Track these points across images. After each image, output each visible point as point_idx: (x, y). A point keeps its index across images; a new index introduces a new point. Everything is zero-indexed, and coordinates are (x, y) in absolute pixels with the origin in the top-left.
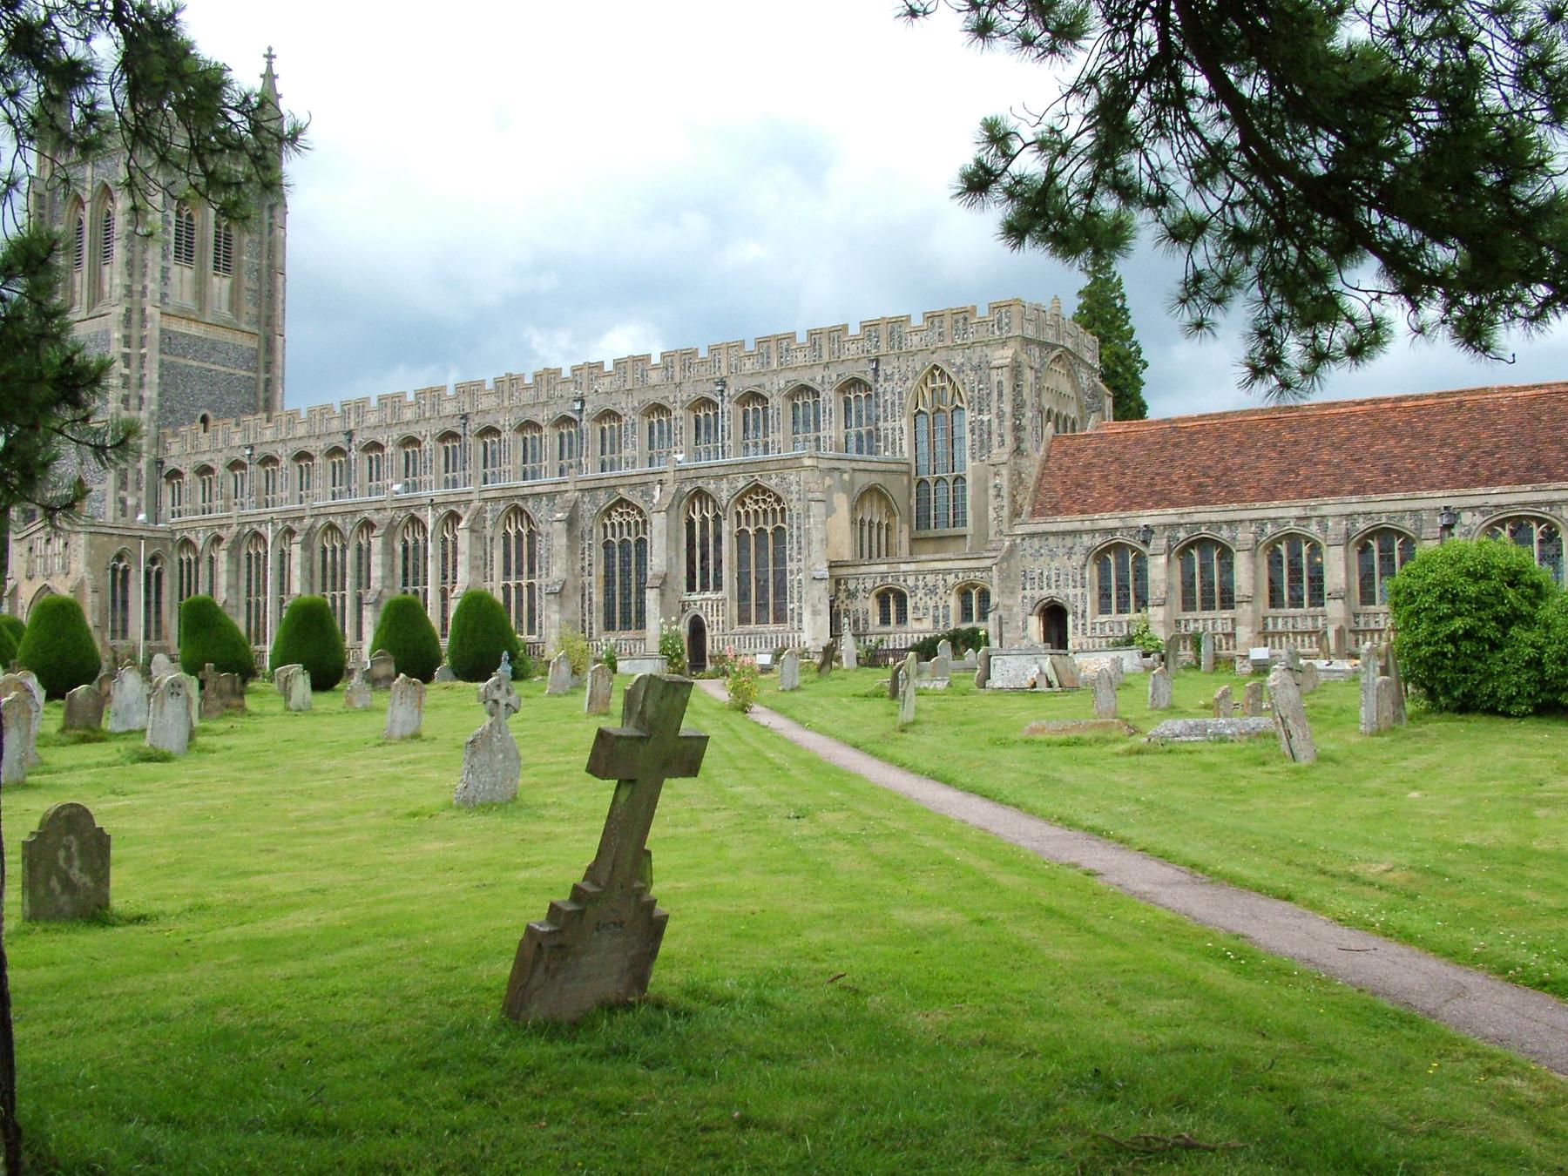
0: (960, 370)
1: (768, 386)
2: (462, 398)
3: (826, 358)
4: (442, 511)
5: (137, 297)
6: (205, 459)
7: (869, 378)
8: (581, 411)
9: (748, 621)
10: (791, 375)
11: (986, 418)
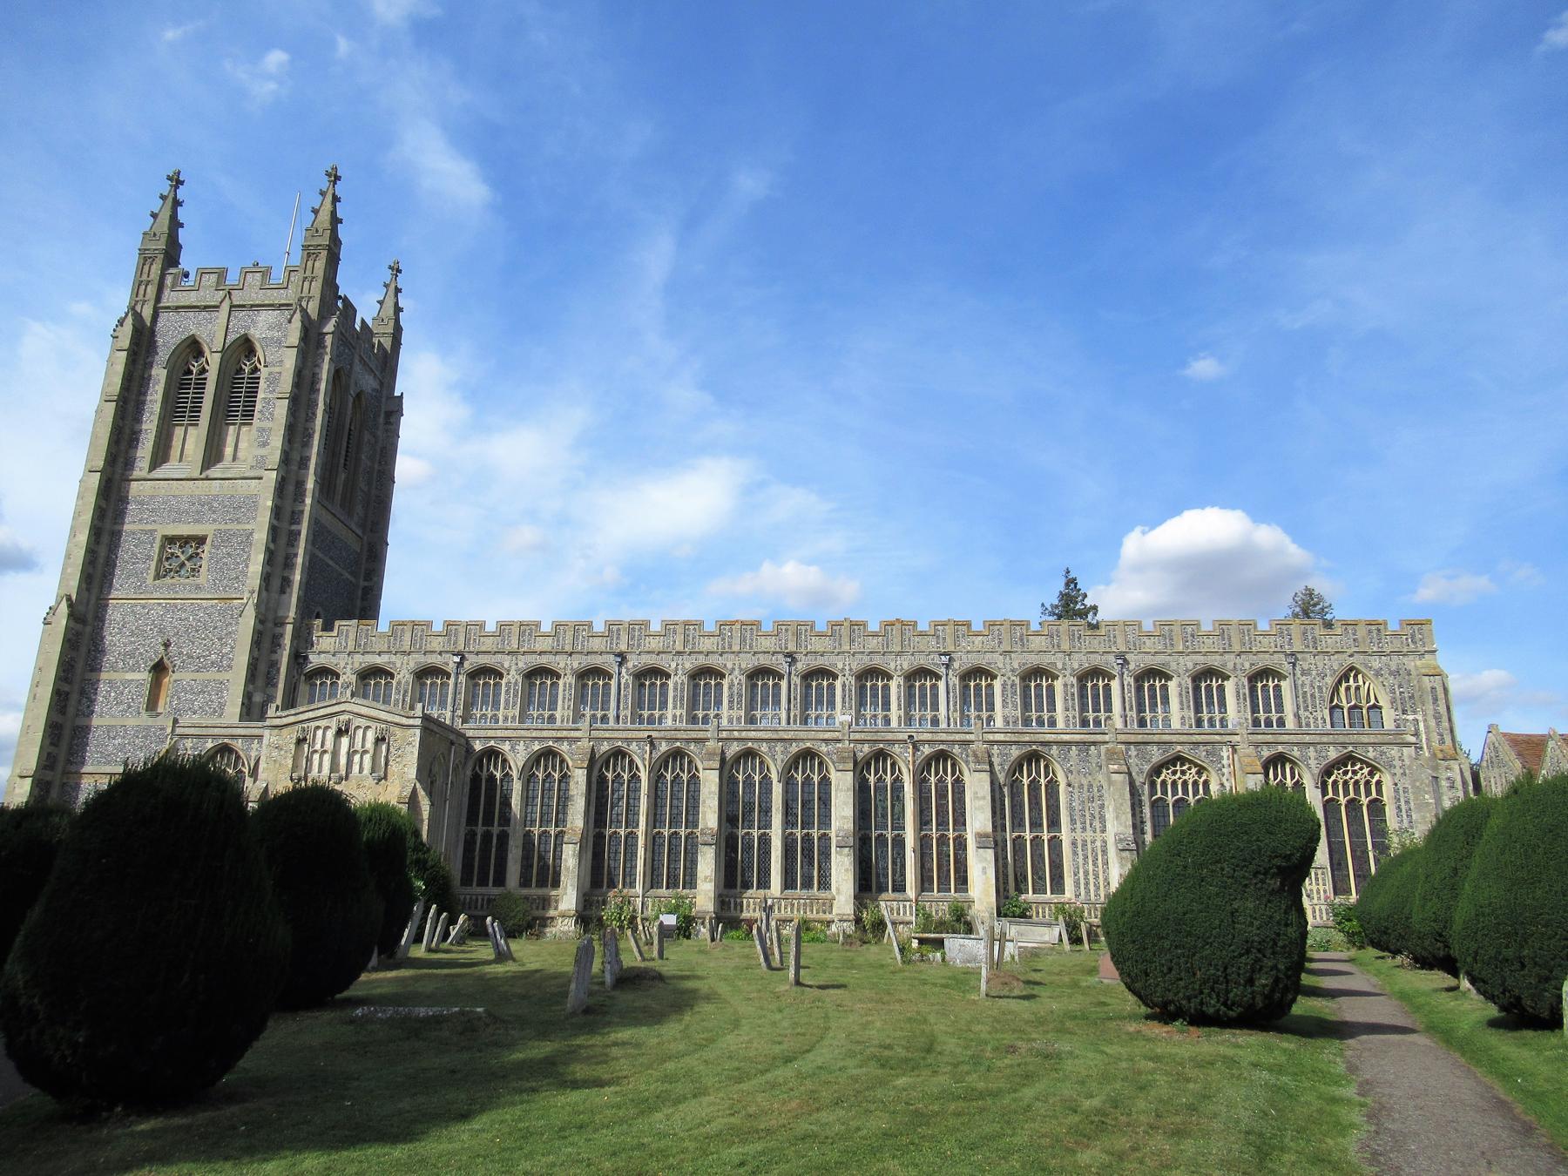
0: (1378, 674)
1: (1174, 666)
2: (782, 635)
3: (1237, 648)
4: (927, 750)
5: (294, 468)
6: (379, 660)
7: (1286, 668)
8: (948, 666)
9: (676, 886)
10: (1200, 659)
11: (1411, 717)
